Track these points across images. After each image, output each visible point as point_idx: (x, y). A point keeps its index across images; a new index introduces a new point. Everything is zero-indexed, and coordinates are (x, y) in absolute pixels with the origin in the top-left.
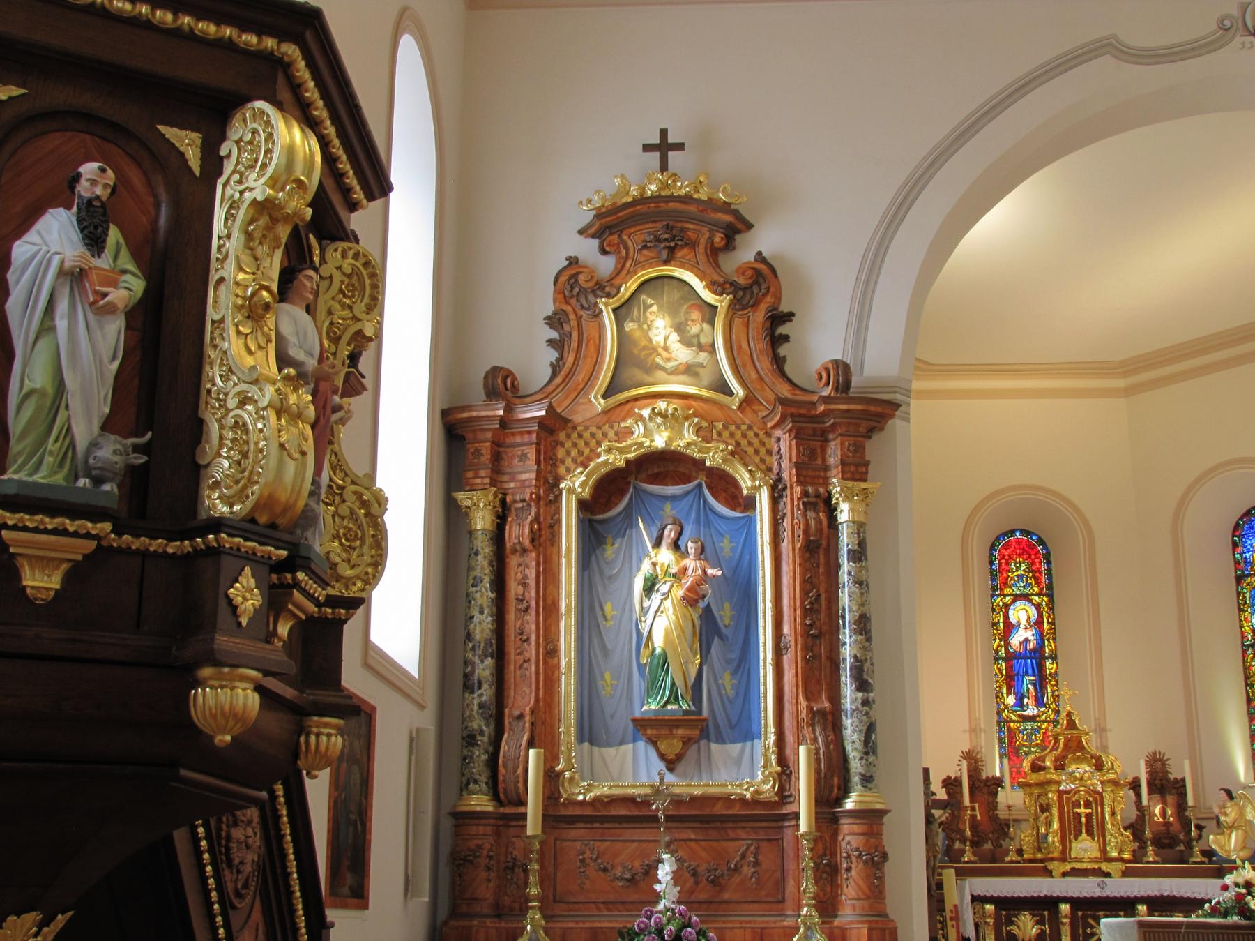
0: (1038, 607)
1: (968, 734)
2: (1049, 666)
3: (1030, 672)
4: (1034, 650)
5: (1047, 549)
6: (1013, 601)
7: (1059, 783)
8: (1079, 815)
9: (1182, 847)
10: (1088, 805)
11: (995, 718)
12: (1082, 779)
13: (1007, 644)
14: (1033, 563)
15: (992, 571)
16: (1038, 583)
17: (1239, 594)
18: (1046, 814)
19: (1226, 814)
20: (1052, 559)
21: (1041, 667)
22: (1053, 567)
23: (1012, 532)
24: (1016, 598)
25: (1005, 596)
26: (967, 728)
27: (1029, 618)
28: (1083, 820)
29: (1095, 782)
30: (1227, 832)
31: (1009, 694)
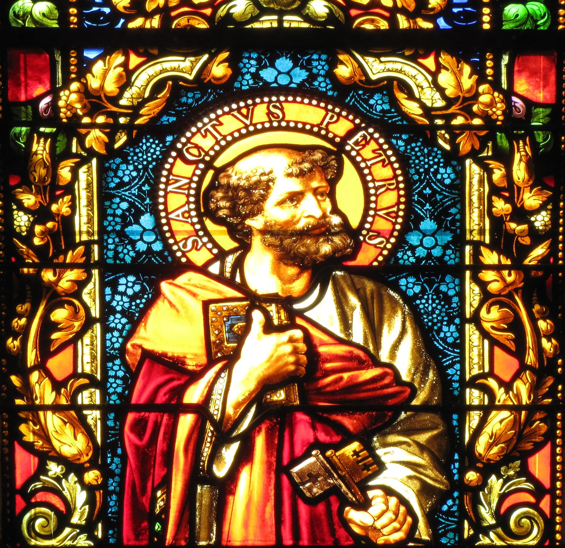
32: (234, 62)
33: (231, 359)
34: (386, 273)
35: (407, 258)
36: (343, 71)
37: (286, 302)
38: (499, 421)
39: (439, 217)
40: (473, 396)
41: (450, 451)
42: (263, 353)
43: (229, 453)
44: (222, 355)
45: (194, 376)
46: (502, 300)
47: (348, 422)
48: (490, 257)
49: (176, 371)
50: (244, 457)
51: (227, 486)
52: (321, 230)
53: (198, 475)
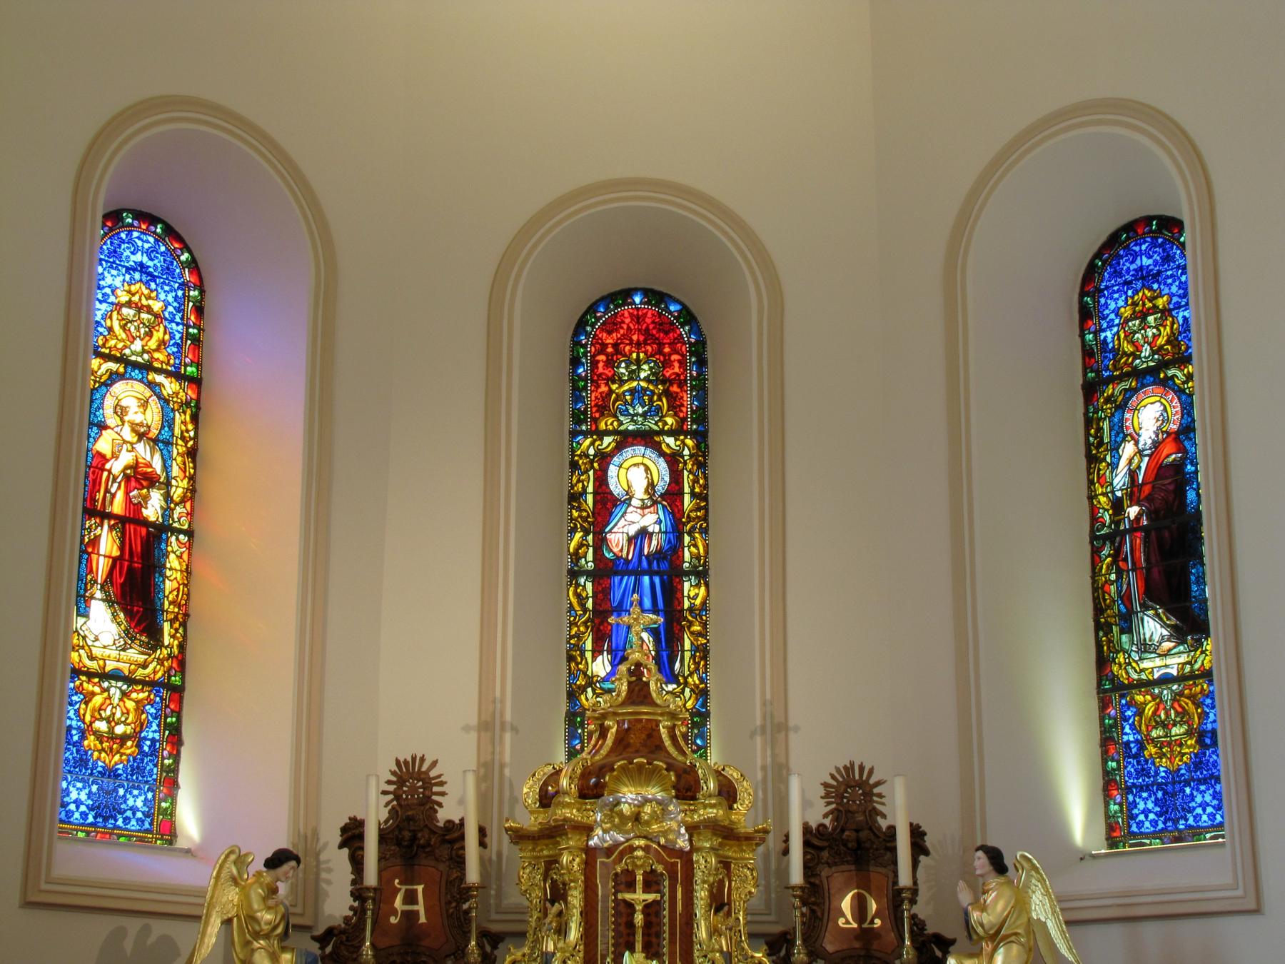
0: (673, 460)
1: (474, 735)
2: (691, 592)
3: (647, 603)
4: (659, 555)
6: (619, 447)
7: (588, 830)
8: (630, 906)
10: (651, 883)
11: (563, 706)
12: (637, 818)
13: (601, 542)
14: (667, 363)
16: (675, 407)
17: (1088, 422)
18: (557, 907)
19: (983, 909)
20: (709, 355)
21: (671, 593)
22: (710, 372)
23: (627, 294)
24: (626, 439)
25: (601, 435)
26: (474, 721)
27: (651, 485)
28: (639, 918)
29: (674, 827)
30: (987, 947)
31: (597, 651)
32: (125, 368)
33: (117, 458)
34: (155, 441)
35: (161, 438)
36: (150, 377)
37: (132, 444)
38: (180, 491)
39: (169, 427)
40: (174, 482)
41: (168, 497)
42: (126, 458)
43: (116, 485)
44: (115, 456)
45: (108, 461)
46: (182, 455)
47: (144, 483)
48: (180, 442)
49: (102, 458)
50: (119, 488)
51: (113, 496)
52: (141, 425)
53: (107, 491)
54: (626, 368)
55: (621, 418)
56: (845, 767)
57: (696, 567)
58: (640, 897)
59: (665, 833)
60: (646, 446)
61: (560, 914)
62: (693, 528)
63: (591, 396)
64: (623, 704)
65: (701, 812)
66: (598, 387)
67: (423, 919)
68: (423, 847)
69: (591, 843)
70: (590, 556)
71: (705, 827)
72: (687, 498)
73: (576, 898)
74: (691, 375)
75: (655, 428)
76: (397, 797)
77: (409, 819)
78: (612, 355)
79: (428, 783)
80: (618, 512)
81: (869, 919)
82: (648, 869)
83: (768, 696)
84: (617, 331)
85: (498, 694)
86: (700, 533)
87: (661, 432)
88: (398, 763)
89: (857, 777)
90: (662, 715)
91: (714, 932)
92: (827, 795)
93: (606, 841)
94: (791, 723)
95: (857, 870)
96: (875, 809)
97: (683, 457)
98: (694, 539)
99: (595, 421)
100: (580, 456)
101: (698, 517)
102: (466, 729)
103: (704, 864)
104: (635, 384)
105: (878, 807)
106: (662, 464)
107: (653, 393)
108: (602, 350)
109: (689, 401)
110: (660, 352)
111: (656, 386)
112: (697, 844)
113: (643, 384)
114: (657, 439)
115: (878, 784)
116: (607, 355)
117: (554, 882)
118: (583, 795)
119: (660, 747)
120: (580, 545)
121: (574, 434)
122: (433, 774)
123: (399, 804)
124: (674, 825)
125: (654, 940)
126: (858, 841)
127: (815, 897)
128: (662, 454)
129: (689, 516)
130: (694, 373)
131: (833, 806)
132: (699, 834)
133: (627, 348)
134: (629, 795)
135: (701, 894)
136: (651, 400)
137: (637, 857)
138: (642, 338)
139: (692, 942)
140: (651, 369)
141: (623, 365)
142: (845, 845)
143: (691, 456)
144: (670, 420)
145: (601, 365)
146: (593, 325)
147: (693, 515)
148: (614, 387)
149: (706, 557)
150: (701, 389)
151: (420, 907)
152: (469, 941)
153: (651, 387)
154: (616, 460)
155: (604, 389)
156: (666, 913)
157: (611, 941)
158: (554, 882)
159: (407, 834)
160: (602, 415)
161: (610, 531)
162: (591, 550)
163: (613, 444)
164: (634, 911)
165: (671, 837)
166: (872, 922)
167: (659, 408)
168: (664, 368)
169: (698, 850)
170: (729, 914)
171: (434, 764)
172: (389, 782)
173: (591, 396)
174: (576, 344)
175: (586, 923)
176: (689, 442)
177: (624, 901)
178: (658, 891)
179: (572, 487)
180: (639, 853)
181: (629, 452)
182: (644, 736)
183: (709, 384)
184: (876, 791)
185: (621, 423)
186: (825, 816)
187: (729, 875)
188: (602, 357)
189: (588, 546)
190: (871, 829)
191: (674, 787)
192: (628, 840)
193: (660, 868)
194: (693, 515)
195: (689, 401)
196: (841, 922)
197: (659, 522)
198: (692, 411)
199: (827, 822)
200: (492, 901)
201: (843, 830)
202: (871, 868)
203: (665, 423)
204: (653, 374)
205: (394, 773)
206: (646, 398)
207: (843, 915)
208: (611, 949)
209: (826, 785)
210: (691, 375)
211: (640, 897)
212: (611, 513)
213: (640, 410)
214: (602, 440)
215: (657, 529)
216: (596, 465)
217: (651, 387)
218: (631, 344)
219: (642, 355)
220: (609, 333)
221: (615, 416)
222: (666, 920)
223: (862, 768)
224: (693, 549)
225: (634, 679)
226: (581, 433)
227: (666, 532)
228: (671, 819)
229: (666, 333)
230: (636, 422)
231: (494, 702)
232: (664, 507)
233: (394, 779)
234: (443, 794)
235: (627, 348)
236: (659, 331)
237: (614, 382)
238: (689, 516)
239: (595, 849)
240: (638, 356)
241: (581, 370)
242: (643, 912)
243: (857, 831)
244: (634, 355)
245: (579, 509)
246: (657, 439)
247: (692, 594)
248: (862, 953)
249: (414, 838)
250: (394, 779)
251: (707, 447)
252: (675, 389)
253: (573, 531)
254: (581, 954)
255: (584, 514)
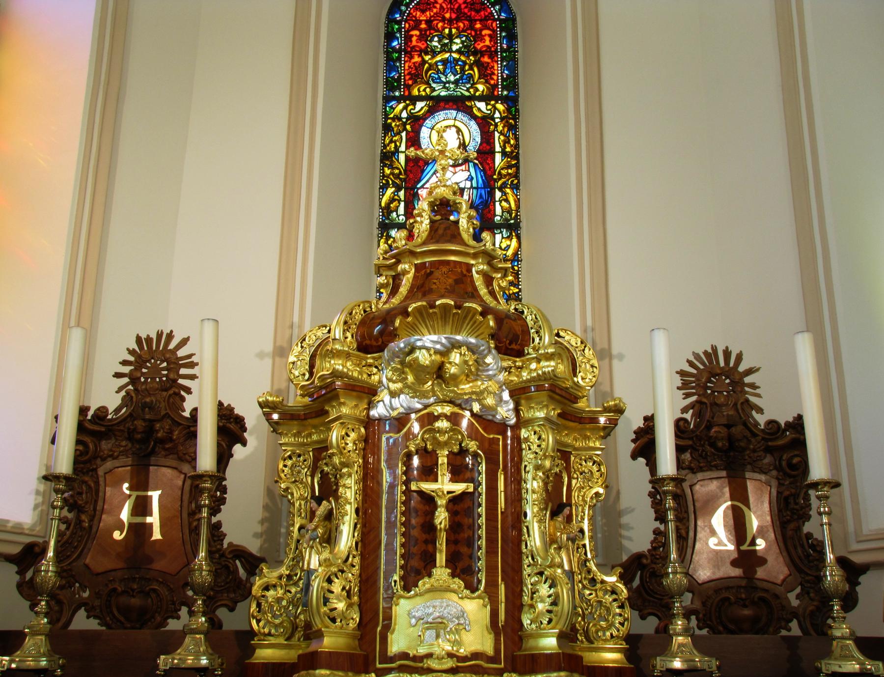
0: (484, 123)
1: (268, 362)
5: (509, 11)
7: (369, 393)
9: (795, 629)
10: (458, 472)
14: (479, 37)
15: (389, 52)
16: (486, 74)
20: (519, 30)
22: (520, 46)
24: (437, 104)
25: (414, 100)
26: (269, 348)
29: (493, 389)
54: (439, 41)
55: (434, 85)
56: (706, 353)
57: (507, 220)
58: (445, 485)
59: (479, 396)
60: (458, 110)
61: (329, 516)
62: (504, 186)
63: (405, 66)
64: (424, 243)
65: (533, 366)
66: (412, 57)
67: (157, 535)
68: (162, 441)
69: (374, 413)
70: (401, 210)
71: (539, 388)
72: (498, 157)
73: (350, 489)
74: (502, 47)
75: (467, 94)
76: (134, 380)
77: (145, 405)
78: (425, 30)
79: (175, 363)
80: (430, 170)
81: (749, 539)
82: (456, 449)
83: (589, 323)
84: (430, 10)
85: (296, 319)
86: (512, 189)
87: (472, 98)
88: (139, 340)
89: (722, 364)
90: (475, 256)
91: (550, 541)
92: (685, 386)
93: (393, 409)
94: (615, 351)
95: (728, 477)
96: (747, 401)
97: (493, 119)
98: (505, 194)
99: (408, 87)
100: (393, 119)
101: (508, 174)
102: (261, 355)
103: (538, 444)
104: (447, 55)
105: (752, 399)
106: (474, 125)
107: (465, 63)
108: (416, 26)
109: (499, 70)
110: (472, 27)
111: (468, 57)
112: (526, 414)
113: (455, 56)
114: (469, 104)
115: (750, 372)
116: (420, 30)
117: (324, 476)
118: (364, 347)
119: (474, 295)
120: (392, 200)
121: (387, 99)
122: (181, 353)
123: (136, 390)
124: (493, 386)
125: (464, 550)
126: (730, 439)
127: (676, 508)
128: (473, 117)
129: (500, 173)
130: (505, 46)
131: (694, 398)
132: (529, 399)
133: (440, 25)
134: (428, 342)
135: (533, 484)
136: (463, 70)
137: (439, 431)
138: (454, 16)
139: (521, 553)
140: (462, 42)
141: (436, 39)
142: (713, 445)
143: (502, 119)
144: (481, 87)
145: (414, 39)
146: (407, 5)
147: (504, 172)
148: (427, 58)
149: (517, 211)
150: (512, 61)
151: (154, 519)
152: (195, 553)
153: (463, 58)
154: (429, 123)
155: (417, 59)
156: (482, 510)
157: (399, 551)
158: (324, 476)
159: (140, 424)
160: (415, 82)
161: (422, 187)
162: (402, 204)
163: (426, 108)
164: (435, 507)
165: (490, 401)
166: (753, 543)
167: (471, 77)
168: (475, 41)
169: (528, 423)
170: (569, 519)
171: (184, 342)
172: (125, 363)
173: (405, 66)
174: (390, 20)
175: (364, 525)
176: (500, 106)
177: (421, 493)
178: (471, 480)
179: (385, 146)
180: (443, 424)
181: (441, 115)
182: (450, 281)
183: (519, 55)
184: (747, 380)
185: (433, 90)
186: (684, 410)
187: (568, 469)
188: (417, 33)
189: (399, 201)
190: (745, 424)
191: (492, 336)
192: (426, 407)
193: (472, 446)
194: (504, 172)
195: (499, 70)
196: (712, 542)
197: (470, 179)
198: (503, 80)
199: (688, 416)
200: (282, 540)
201: (709, 427)
202: (748, 475)
203: (477, 90)
204: (465, 47)
205: (132, 352)
206: (458, 68)
207: (713, 533)
208: (399, 562)
209: (682, 373)
210: (502, 47)
211: (445, 485)
212: (423, 171)
213: (452, 78)
214: (414, 105)
215: (468, 184)
216: (408, 127)
217: (463, 58)
218: (443, 19)
219: (454, 31)
220: (423, 12)
221: (428, 83)
222: (483, 520)
223: (727, 353)
224: (504, 204)
225: (438, 217)
226: (394, 98)
227: (477, 188)
228: (490, 378)
229: (478, 11)
230: (448, 89)
231: (292, 327)
232: (475, 165)
233: (132, 359)
234: (193, 377)
235: (440, 25)
236: (471, 9)
237: (427, 54)
238: (500, 173)
239: (381, 420)
240: (450, 31)
241: (395, 43)
242: (448, 509)
243: (728, 426)
244: (447, 31)
245: (391, 167)
246: (469, 104)
247: (504, 246)
248: (743, 583)
249: (150, 430)
250: (132, 359)
251: (517, 110)
252: (486, 59)
253: (384, 187)
254: (356, 570)
255: (397, 171)
